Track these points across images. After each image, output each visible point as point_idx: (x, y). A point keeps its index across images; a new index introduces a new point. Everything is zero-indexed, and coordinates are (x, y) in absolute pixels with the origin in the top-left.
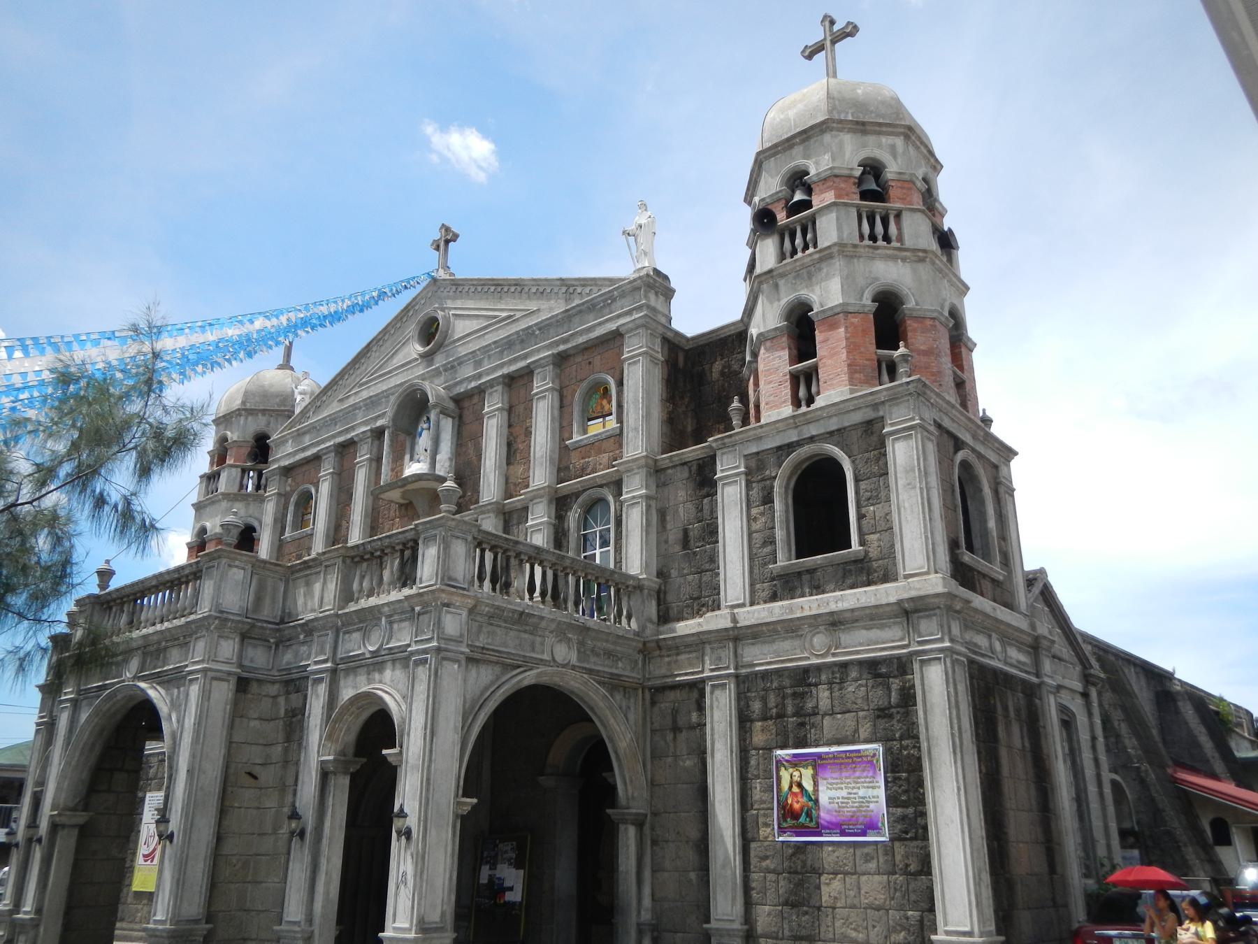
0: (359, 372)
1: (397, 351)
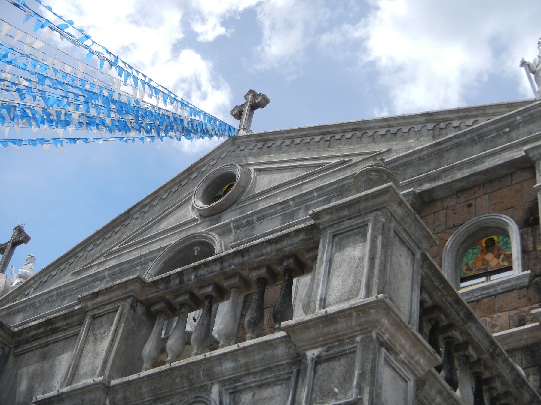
0: (108, 242)
1: (167, 215)
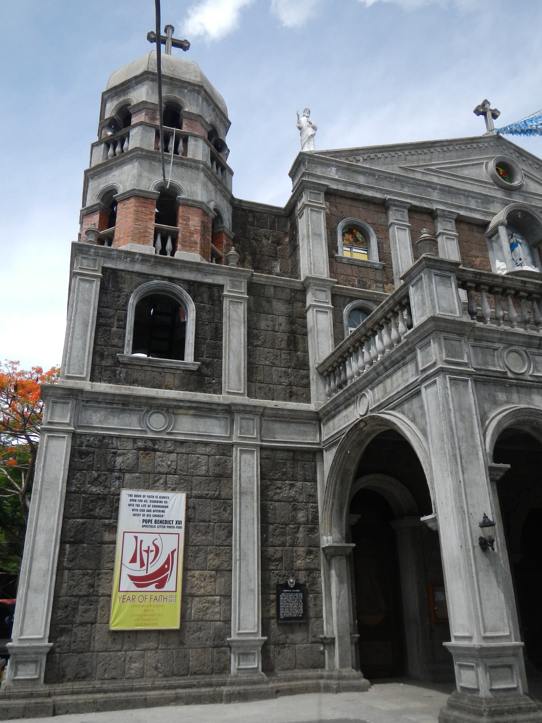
0: (422, 157)
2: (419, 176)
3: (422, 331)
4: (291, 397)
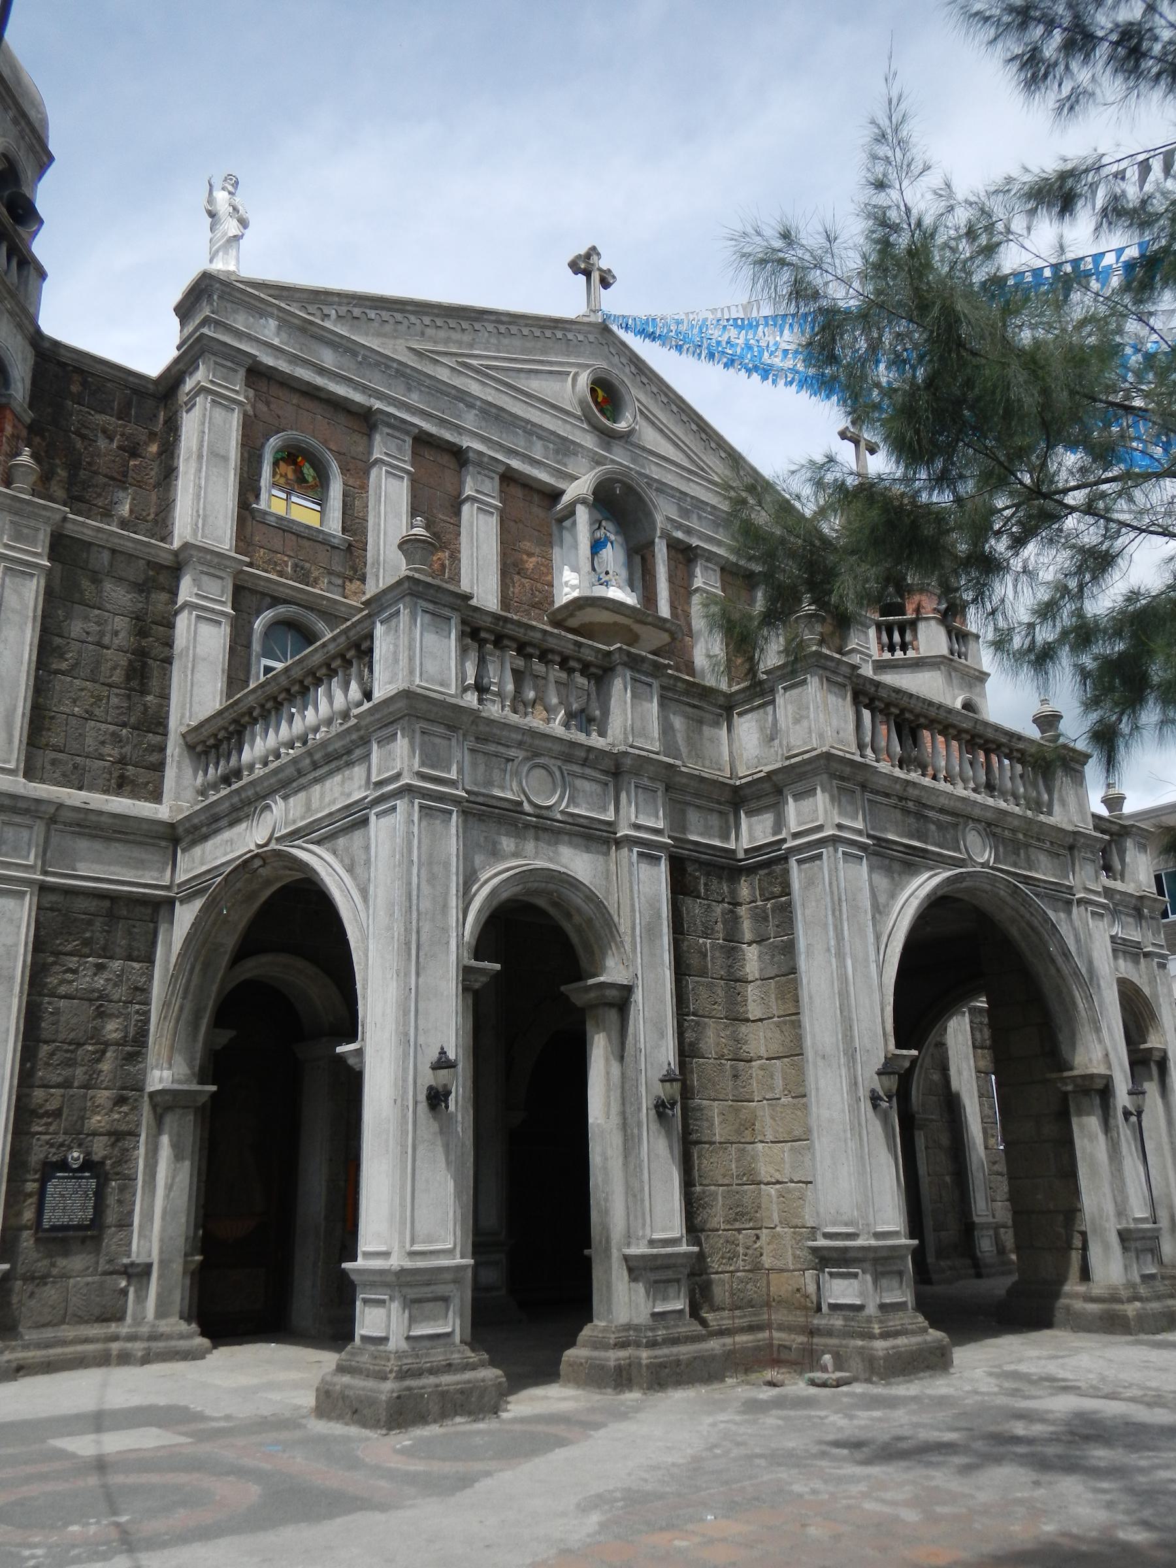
0: (456, 336)
2: (443, 374)
3: (386, 711)
4: (120, 786)
